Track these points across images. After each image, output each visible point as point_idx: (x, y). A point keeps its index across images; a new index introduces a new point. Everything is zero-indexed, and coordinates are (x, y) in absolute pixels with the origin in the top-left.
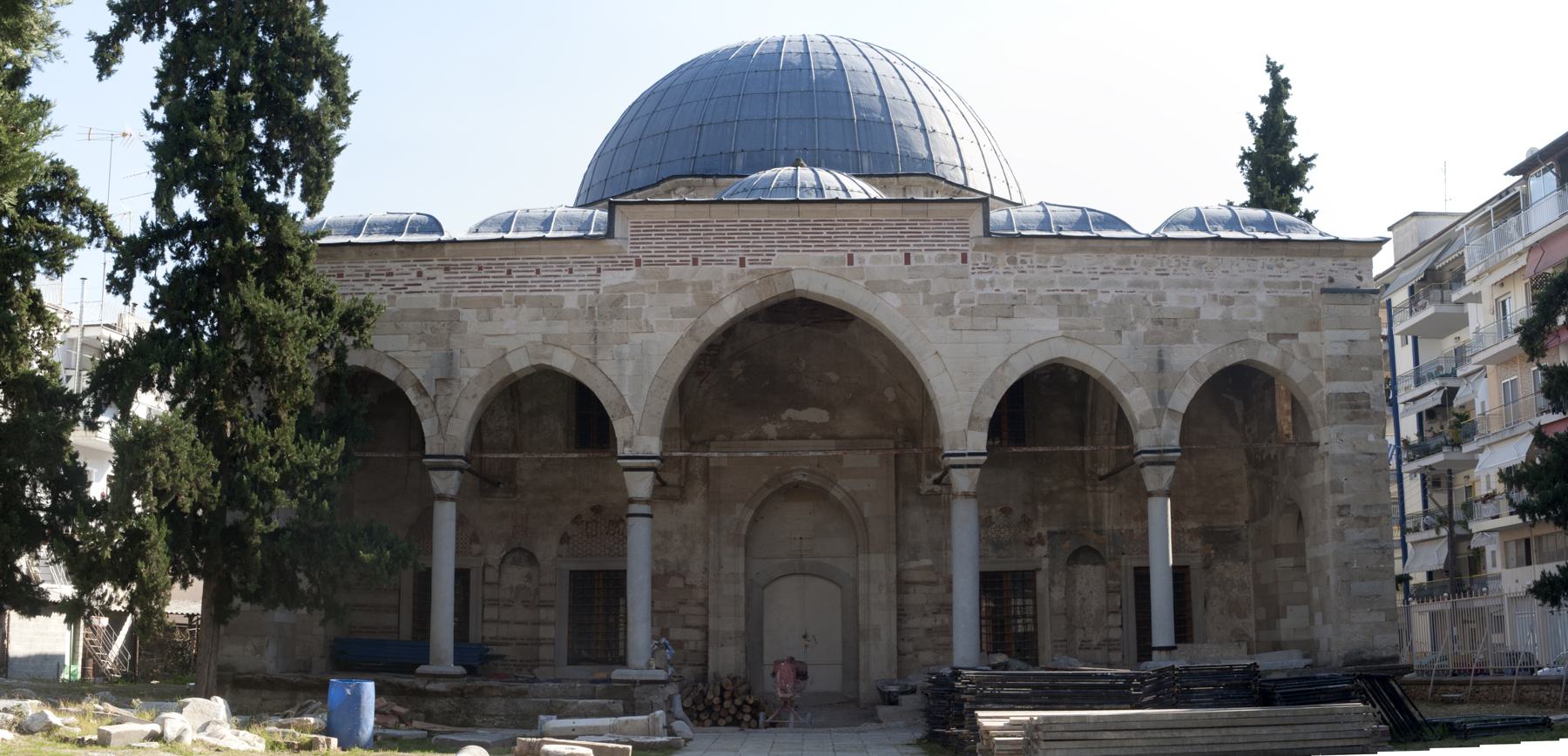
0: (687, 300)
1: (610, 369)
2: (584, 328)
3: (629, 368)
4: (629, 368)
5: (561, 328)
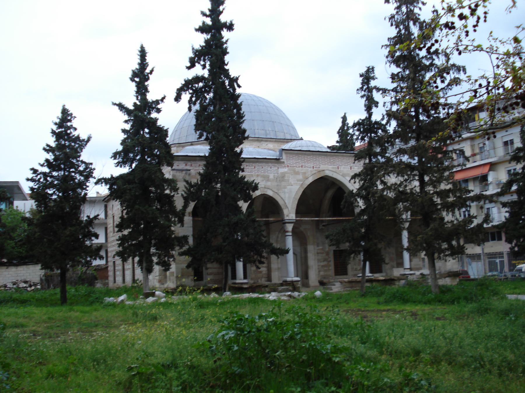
0: (300, 177)
1: (282, 195)
2: (275, 184)
3: (287, 195)
4: (287, 195)
5: (269, 184)
